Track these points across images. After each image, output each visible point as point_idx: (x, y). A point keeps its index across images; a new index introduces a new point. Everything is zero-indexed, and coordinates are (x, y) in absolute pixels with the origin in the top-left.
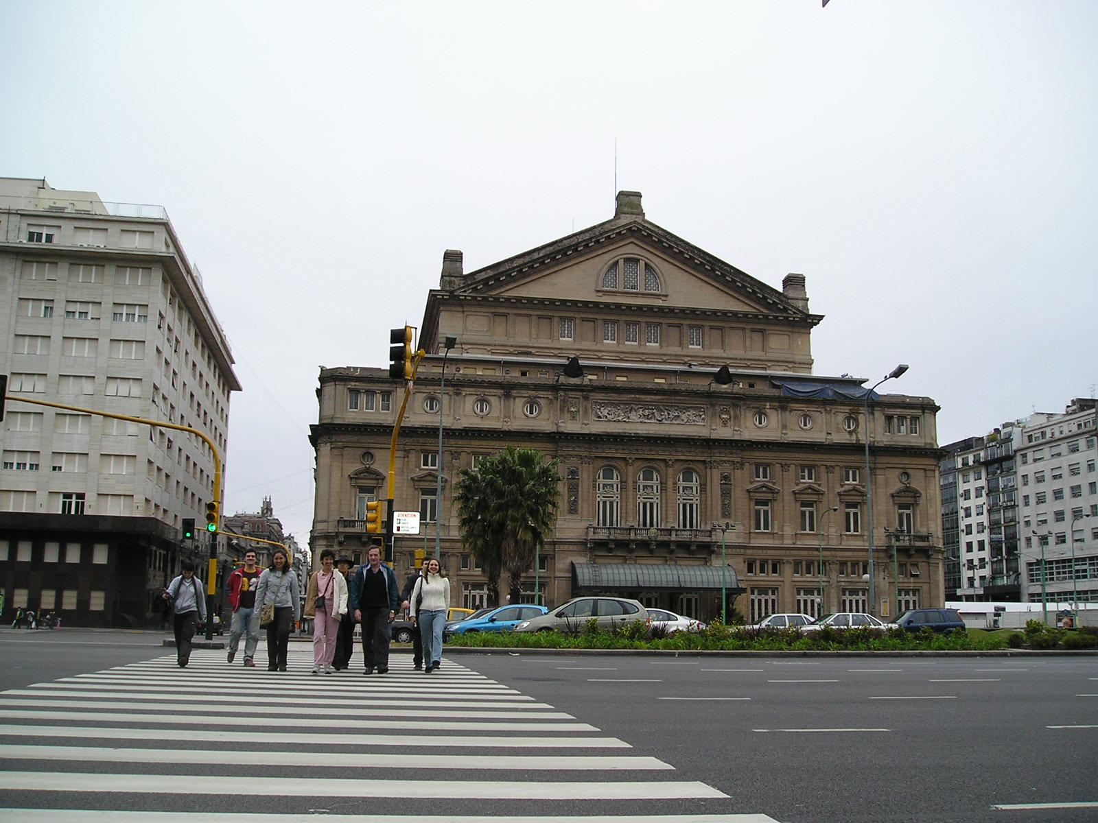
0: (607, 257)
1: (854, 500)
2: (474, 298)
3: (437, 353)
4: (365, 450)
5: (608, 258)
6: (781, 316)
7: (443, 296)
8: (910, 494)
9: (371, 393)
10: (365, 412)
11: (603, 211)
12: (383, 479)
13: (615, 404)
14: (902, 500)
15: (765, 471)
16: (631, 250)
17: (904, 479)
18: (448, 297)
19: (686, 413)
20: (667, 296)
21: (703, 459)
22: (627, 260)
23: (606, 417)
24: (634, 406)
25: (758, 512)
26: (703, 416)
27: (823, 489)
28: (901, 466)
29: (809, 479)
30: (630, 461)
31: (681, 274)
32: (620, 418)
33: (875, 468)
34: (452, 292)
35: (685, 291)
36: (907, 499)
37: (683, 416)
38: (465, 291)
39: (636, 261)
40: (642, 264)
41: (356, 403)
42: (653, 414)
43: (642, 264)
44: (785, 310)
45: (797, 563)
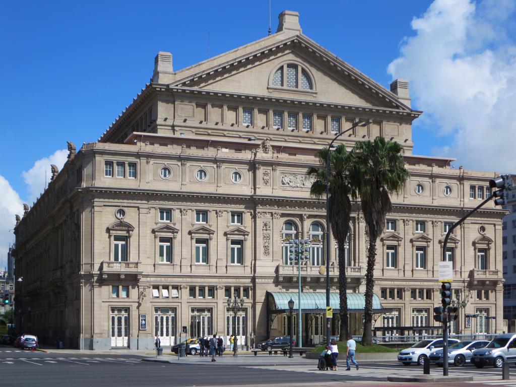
3: (156, 132)
4: (118, 208)
7: (161, 88)
9: (121, 164)
10: (117, 178)
12: (133, 231)
17: (482, 233)
18: (164, 90)
20: (316, 93)
22: (289, 66)
23: (289, 184)
30: (305, 217)
31: (327, 79)
34: (168, 86)
38: (177, 85)
40: (300, 69)
44: (397, 107)
45: (413, 292)
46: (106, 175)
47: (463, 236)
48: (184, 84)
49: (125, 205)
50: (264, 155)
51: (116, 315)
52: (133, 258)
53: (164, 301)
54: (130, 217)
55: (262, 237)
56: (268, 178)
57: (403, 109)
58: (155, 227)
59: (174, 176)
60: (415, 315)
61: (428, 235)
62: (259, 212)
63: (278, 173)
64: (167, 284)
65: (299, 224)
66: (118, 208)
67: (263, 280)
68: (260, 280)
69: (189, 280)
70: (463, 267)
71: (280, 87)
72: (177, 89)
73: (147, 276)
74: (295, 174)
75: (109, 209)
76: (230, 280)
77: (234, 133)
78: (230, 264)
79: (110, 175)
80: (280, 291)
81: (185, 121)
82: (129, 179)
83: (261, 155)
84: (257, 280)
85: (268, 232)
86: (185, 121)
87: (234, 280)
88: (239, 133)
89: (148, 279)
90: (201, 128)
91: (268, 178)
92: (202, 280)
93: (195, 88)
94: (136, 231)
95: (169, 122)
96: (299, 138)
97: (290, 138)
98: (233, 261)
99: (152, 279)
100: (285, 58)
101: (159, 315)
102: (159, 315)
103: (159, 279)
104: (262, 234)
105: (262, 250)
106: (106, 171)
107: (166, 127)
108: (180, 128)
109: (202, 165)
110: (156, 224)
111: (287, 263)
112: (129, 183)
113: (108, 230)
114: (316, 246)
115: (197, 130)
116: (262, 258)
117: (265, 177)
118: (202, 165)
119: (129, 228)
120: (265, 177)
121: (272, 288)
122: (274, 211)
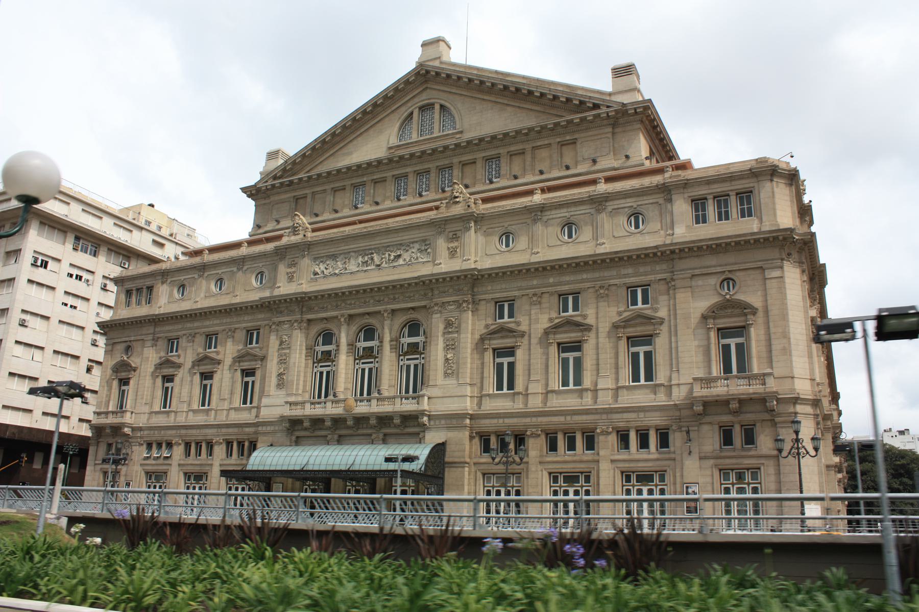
0: (403, 109)
1: (639, 336)
2: (273, 186)
6: (590, 115)
8: (737, 311)
13: (334, 257)
15: (511, 308)
19: (410, 252)
20: (461, 132)
24: (353, 254)
26: (429, 250)
27: (590, 320)
28: (719, 269)
29: (574, 311)
32: (337, 272)
33: (673, 280)
35: (481, 121)
36: (731, 325)
37: (406, 256)
40: (437, 107)
42: (372, 259)
43: (437, 107)
47: (673, 311)
48: (275, 178)
57: (608, 107)
60: (493, 487)
69: (183, 432)
70: (674, 375)
76: (231, 430)
87: (236, 430)
100: (416, 100)
114: (367, 367)
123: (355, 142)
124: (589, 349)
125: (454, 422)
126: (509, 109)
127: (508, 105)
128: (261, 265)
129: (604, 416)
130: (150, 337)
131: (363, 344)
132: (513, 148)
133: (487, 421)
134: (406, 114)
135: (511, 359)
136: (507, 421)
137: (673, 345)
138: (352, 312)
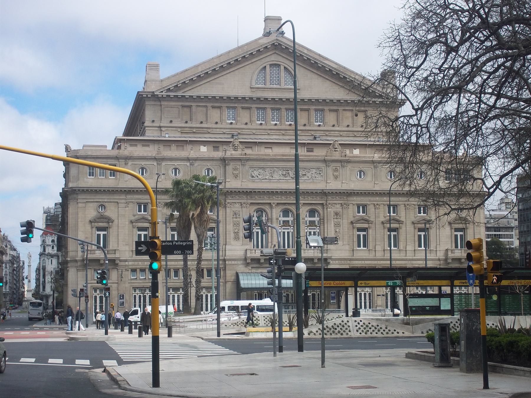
3: (143, 134)
4: (100, 204)
5: (260, 65)
7: (147, 95)
11: (253, 32)
12: (112, 222)
14: (457, 226)
16: (274, 58)
19: (311, 172)
21: (321, 202)
22: (271, 65)
24: (276, 169)
25: (359, 236)
26: (322, 174)
27: (403, 219)
30: (274, 205)
31: (310, 75)
32: (267, 178)
34: (153, 92)
37: (309, 175)
38: (162, 92)
39: (279, 66)
40: (282, 68)
41: (93, 172)
43: (282, 68)
46: (90, 175)
48: (169, 90)
49: (106, 200)
50: (233, 152)
51: (98, 294)
52: (112, 245)
53: (141, 282)
54: (111, 212)
55: (232, 225)
56: (237, 172)
58: (133, 218)
59: (150, 174)
61: (400, 217)
62: (228, 203)
63: (247, 167)
64: (144, 267)
65: (269, 211)
66: (98, 203)
67: (233, 262)
68: (230, 262)
70: (438, 246)
71: (263, 86)
72: (162, 95)
73: (126, 261)
74: (263, 168)
75: (91, 205)
77: (218, 130)
78: (417, 248)
79: (93, 176)
80: (250, 271)
81: (171, 122)
82: (110, 179)
83: (230, 153)
84: (227, 262)
85: (238, 219)
86: (171, 122)
88: (222, 130)
89: (127, 263)
90: (186, 127)
91: (237, 172)
92: (176, 263)
93: (180, 94)
94: (116, 221)
95: (156, 124)
96: (281, 132)
97: (272, 131)
98: (420, 246)
99: (130, 263)
100: (268, 59)
101: (137, 294)
102: (137, 294)
103: (136, 263)
104: (232, 221)
105: (232, 235)
106: (90, 172)
107: (153, 128)
108: (166, 129)
109: (176, 164)
110: (134, 216)
111: (456, 246)
112: (109, 182)
113: (91, 222)
114: (286, 231)
115: (182, 129)
116: (232, 243)
117: (235, 172)
118: (176, 164)
119: (109, 220)
120: (235, 172)
121: (241, 268)
122: (242, 201)
123: (224, 77)
124: (402, 232)
125: (343, 262)
126: (328, 81)
127: (327, 79)
128: (208, 164)
129: (409, 262)
130: (123, 201)
131: (282, 219)
132: (332, 108)
133: (357, 262)
134: (261, 67)
135: (364, 233)
136: (366, 262)
137: (438, 233)
138: (279, 202)
